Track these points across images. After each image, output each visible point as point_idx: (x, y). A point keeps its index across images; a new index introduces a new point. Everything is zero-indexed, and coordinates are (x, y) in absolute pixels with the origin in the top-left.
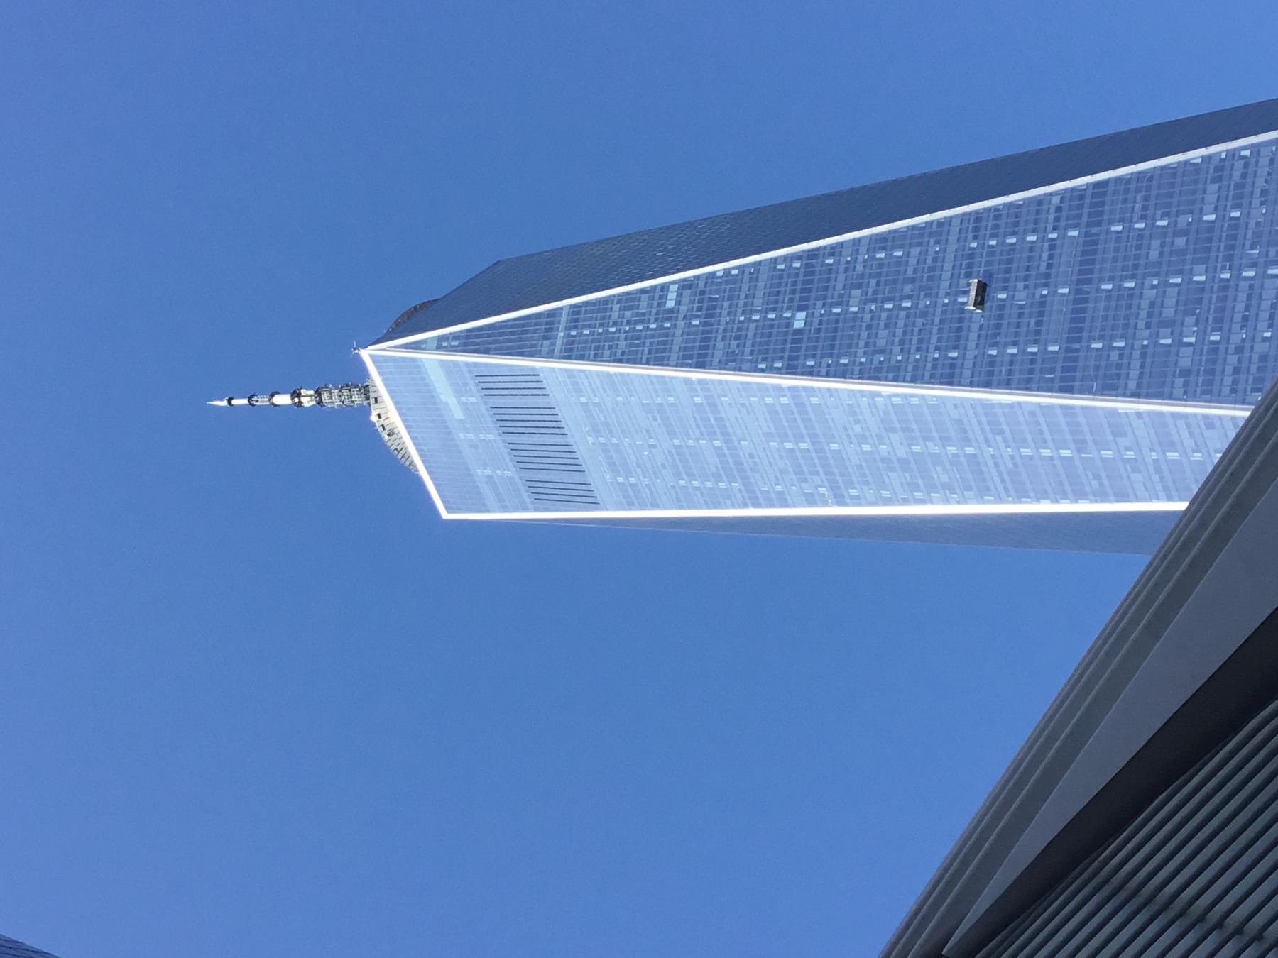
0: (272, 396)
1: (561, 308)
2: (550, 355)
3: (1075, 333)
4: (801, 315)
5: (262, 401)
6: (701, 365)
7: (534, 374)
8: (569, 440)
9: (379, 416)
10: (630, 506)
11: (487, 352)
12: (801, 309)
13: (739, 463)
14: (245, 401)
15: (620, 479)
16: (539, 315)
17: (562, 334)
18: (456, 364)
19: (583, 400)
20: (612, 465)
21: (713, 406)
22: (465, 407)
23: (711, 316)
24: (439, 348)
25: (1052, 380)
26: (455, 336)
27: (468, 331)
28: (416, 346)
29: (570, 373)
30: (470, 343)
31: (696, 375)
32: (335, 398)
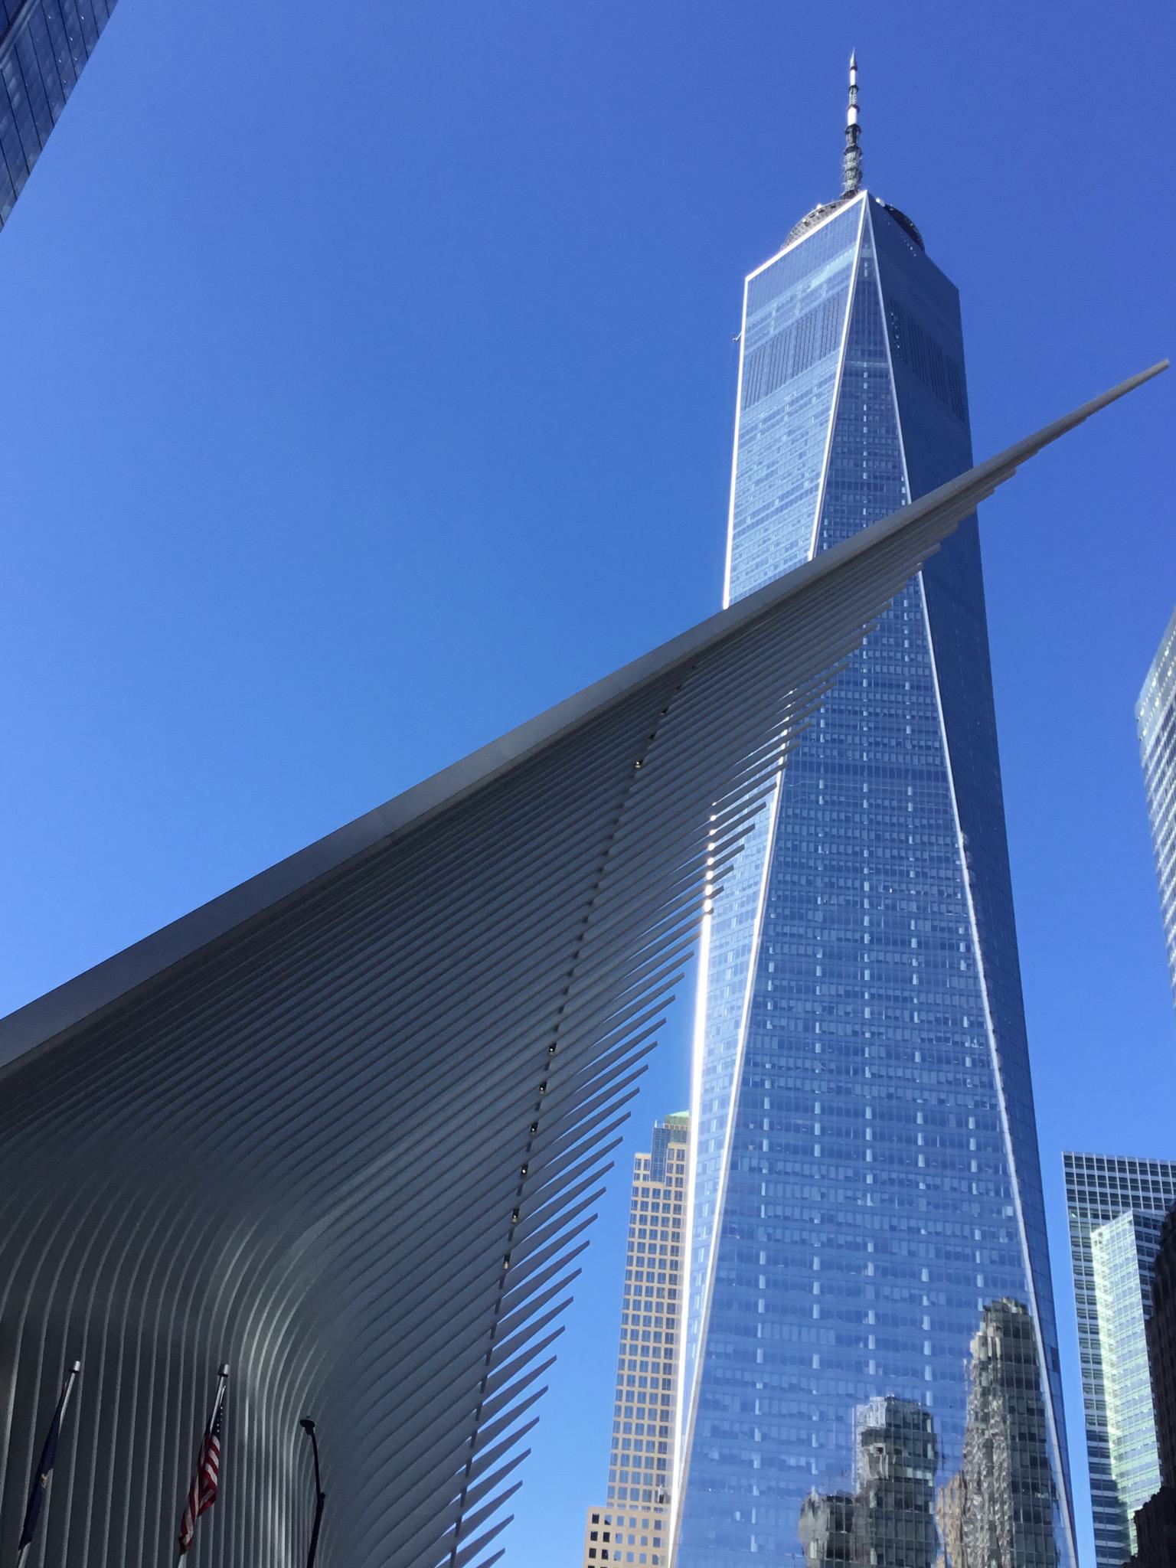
0: (855, 106)
1: (886, 361)
2: (848, 356)
3: (832, 768)
5: (853, 98)
6: (829, 484)
7: (836, 345)
9: (821, 211)
10: (741, 436)
13: (762, 520)
14: (853, 82)
15: (760, 426)
16: (882, 343)
18: (848, 277)
20: (770, 418)
21: (801, 497)
22: (820, 286)
23: (869, 488)
24: (861, 260)
25: (797, 754)
26: (871, 273)
28: (865, 239)
30: (864, 287)
31: (821, 481)
32: (850, 165)
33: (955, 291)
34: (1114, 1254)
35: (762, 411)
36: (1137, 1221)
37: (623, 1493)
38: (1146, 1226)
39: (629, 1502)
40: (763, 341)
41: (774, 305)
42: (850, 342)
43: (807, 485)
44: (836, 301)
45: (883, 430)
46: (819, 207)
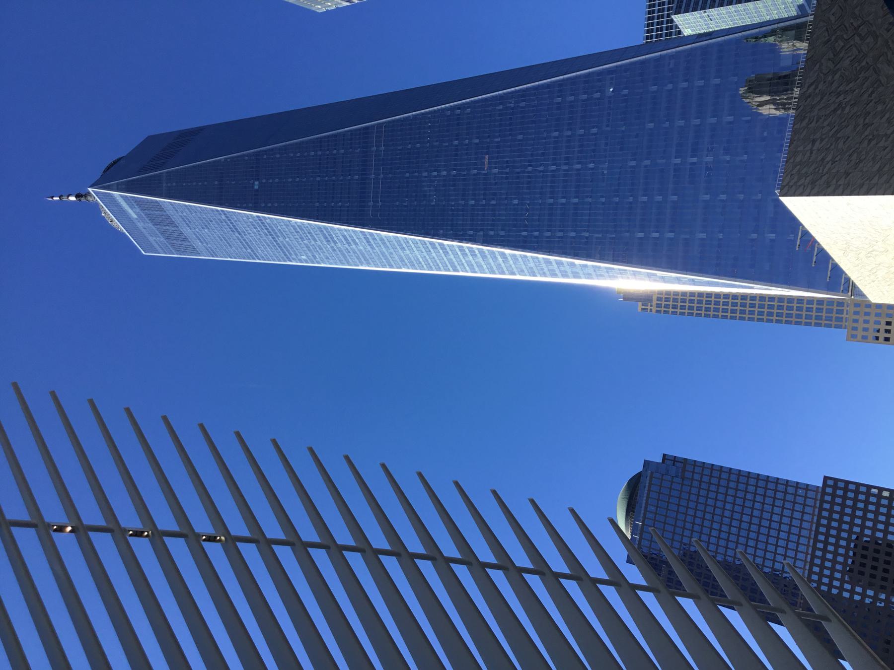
4: (257, 183)
12: (258, 179)
18: (126, 197)
34: (689, 24)
36: (678, 12)
37: (839, 319)
38: (681, 8)
39: (844, 316)
41: (151, 239)
43: (223, 217)
44: (139, 202)
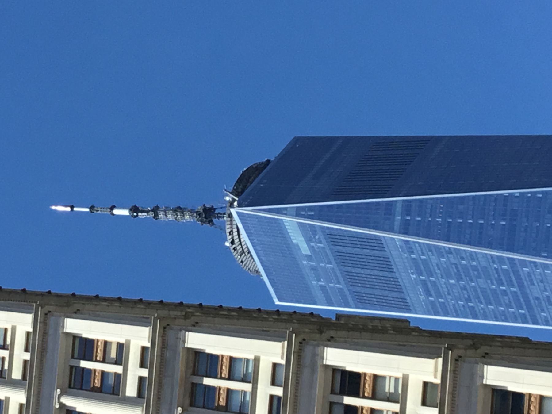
1: (396, 201)
7: (378, 239)
8: (397, 275)
9: (233, 243)
11: (338, 222)
13: (528, 302)
14: (88, 210)
17: (400, 218)
19: (413, 256)
22: (311, 248)
26: (311, 209)
27: (320, 206)
29: (407, 242)
31: (506, 255)
32: (170, 217)
33: (297, 140)
35: (416, 295)
40: (347, 293)
42: (376, 228)
45: (461, 207)
46: (227, 244)
